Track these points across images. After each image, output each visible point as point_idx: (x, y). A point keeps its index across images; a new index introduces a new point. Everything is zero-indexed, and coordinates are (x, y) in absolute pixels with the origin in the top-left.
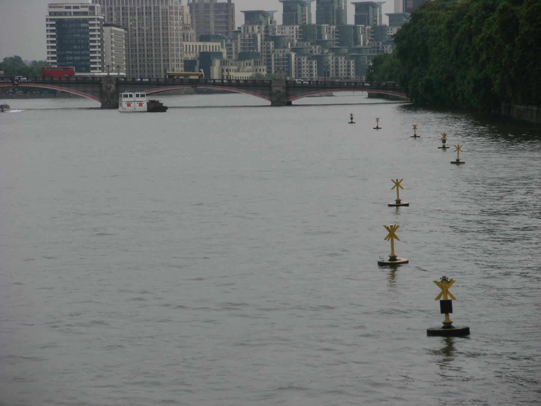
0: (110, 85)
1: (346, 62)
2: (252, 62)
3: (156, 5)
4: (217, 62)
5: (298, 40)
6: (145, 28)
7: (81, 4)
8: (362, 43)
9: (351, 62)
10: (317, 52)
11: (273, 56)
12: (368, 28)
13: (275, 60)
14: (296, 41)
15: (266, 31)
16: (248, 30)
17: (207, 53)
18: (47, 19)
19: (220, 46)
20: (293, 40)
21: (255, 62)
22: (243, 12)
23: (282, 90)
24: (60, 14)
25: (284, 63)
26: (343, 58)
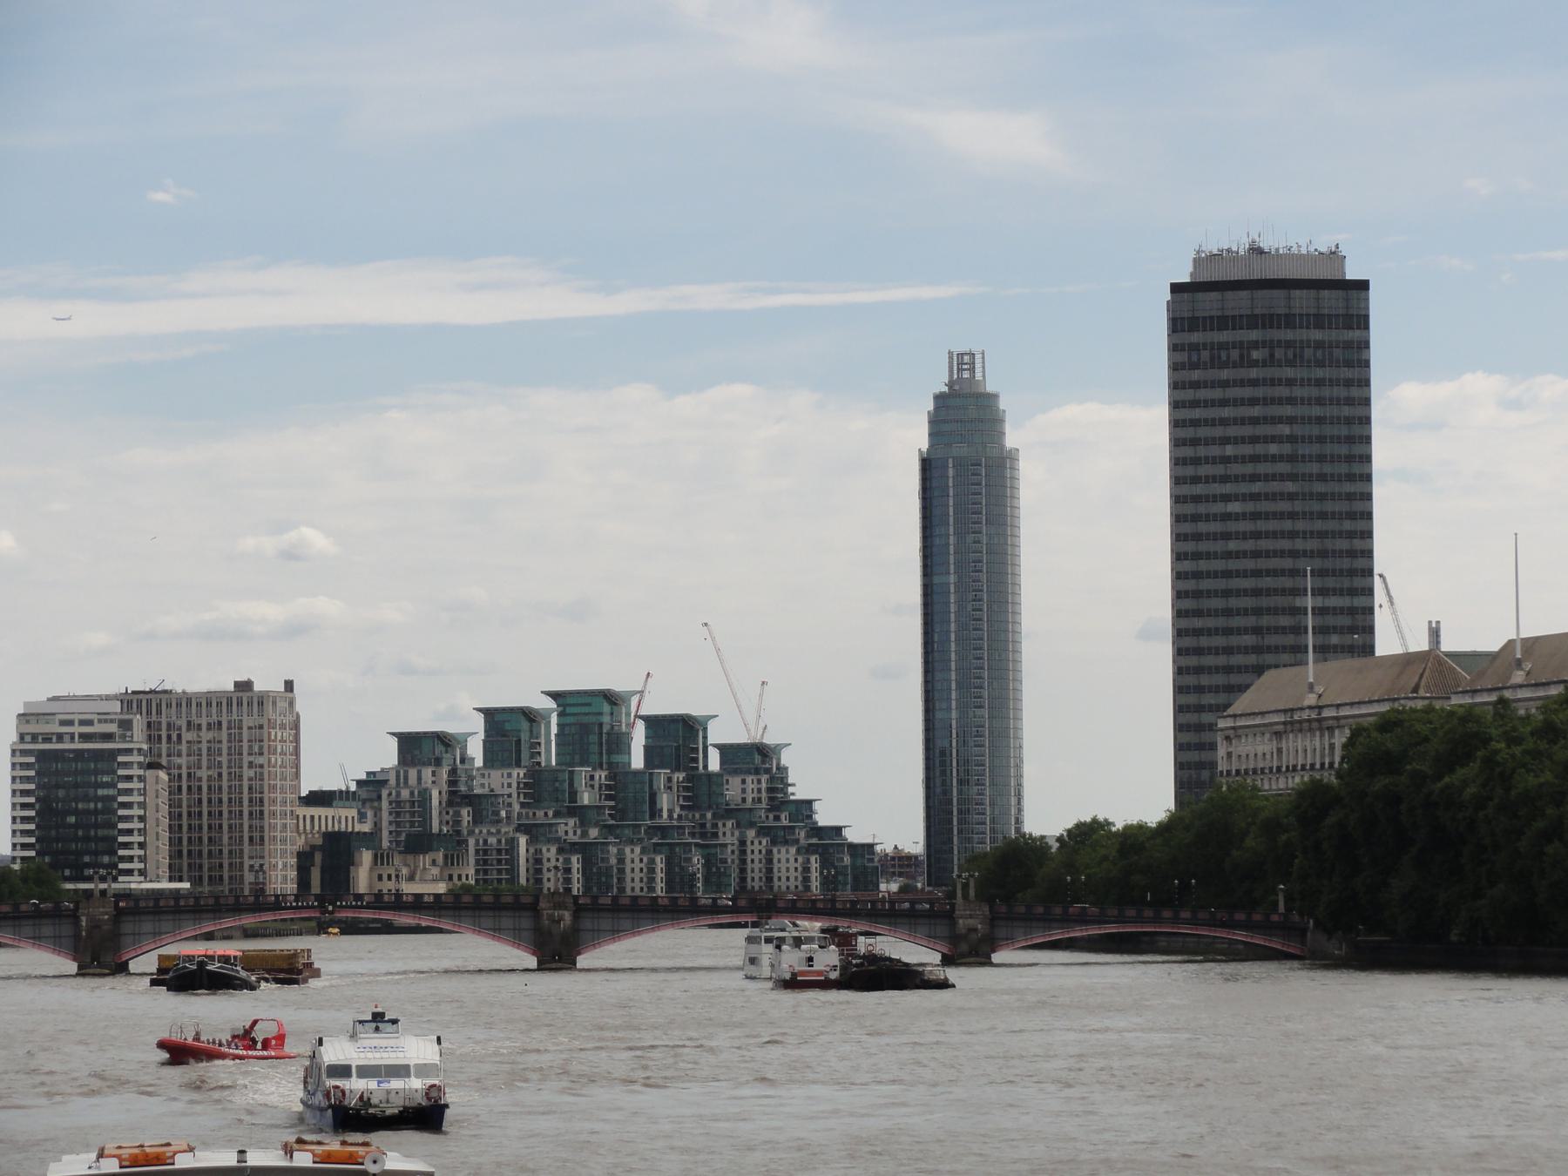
0: (561, 912)
1: (645, 860)
2: (440, 856)
3: (235, 717)
4: (366, 857)
5: (523, 805)
6: (203, 773)
7: (99, 714)
8: (665, 815)
9: (658, 859)
10: (571, 833)
11: (471, 842)
12: (678, 778)
13: (477, 852)
14: (517, 807)
15: (452, 782)
16: (406, 778)
17: (339, 833)
18: (14, 752)
19: (356, 818)
20: (510, 805)
21: (446, 857)
22: (393, 734)
23: (979, 926)
24: (47, 740)
25: (499, 861)
26: (638, 850)
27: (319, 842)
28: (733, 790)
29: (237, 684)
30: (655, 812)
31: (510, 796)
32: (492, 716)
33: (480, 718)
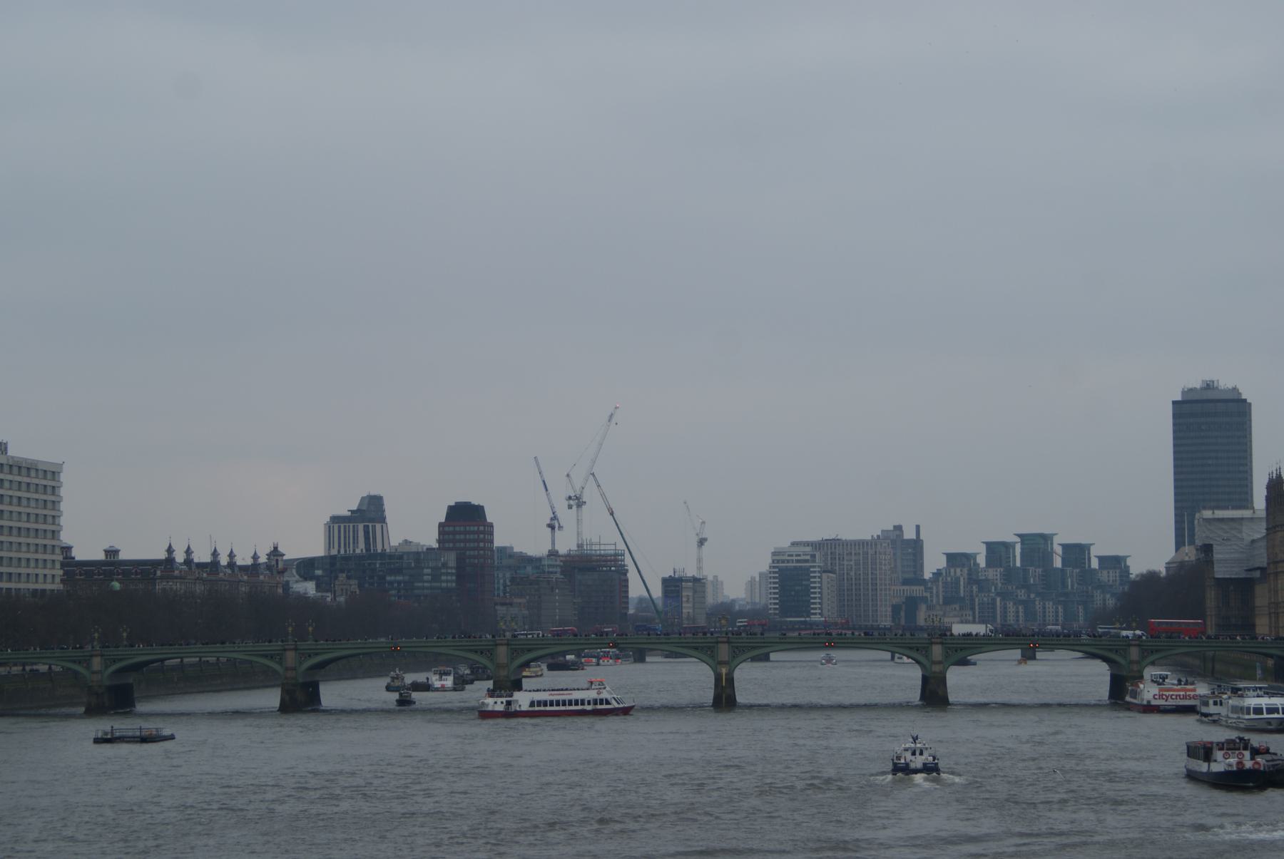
2: (957, 607)
4: (923, 607)
5: (1002, 584)
8: (1070, 587)
11: (977, 600)
13: (979, 604)
14: (1000, 585)
15: (969, 574)
16: (950, 573)
18: (770, 567)
20: (997, 584)
21: (960, 606)
22: (944, 554)
24: (783, 561)
26: (1051, 603)
27: (904, 600)
28: (1105, 576)
29: (895, 527)
30: (1064, 584)
31: (997, 579)
32: (990, 546)
33: (984, 547)
